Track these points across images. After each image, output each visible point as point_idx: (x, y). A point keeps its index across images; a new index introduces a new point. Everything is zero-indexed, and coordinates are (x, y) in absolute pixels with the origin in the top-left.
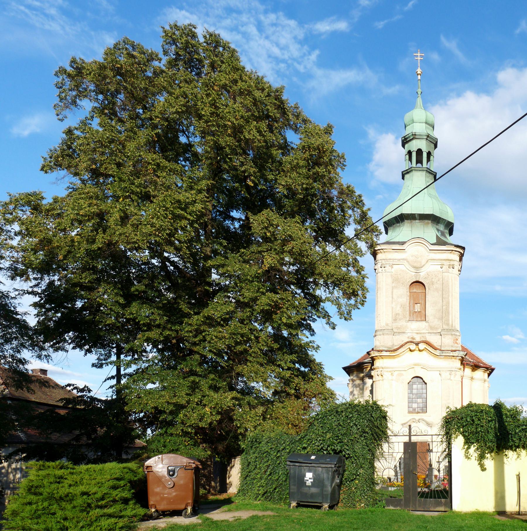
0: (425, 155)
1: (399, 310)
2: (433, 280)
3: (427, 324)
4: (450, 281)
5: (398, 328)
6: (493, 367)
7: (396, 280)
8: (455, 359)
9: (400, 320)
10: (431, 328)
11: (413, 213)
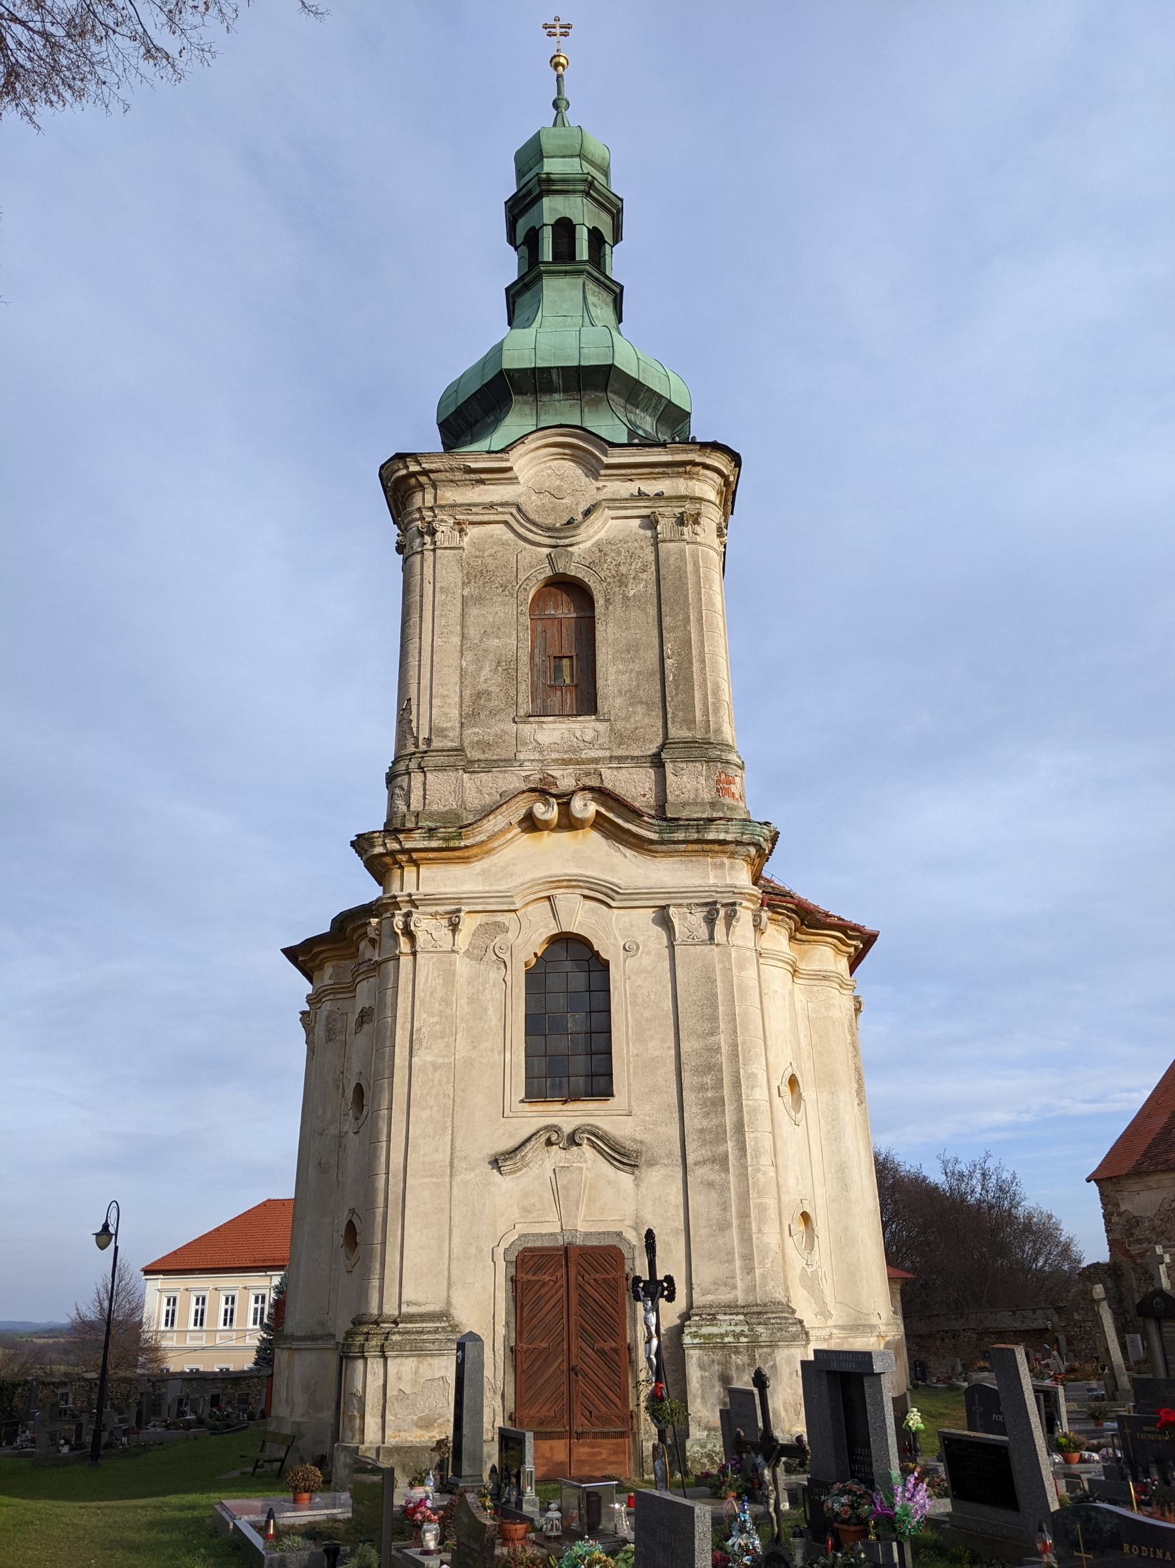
0: (582, 236)
1: (488, 677)
2: (623, 569)
3: (602, 727)
4: (690, 568)
5: (484, 745)
6: (870, 927)
7: (475, 573)
8: (732, 855)
9: (493, 713)
10: (620, 738)
11: (541, 364)
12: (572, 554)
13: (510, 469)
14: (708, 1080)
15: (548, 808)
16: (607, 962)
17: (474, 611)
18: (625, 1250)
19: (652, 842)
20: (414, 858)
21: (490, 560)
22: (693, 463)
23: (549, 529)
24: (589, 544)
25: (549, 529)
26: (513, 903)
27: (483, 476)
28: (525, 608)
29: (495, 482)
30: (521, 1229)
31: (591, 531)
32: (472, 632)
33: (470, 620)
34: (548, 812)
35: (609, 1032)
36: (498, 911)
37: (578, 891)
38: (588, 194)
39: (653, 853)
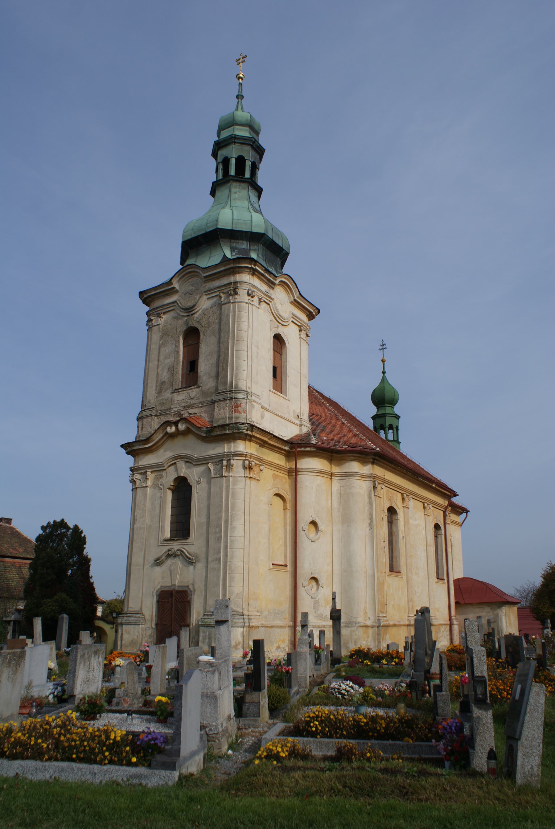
0: (233, 161)
10: (204, 394)
14: (217, 530)
16: (191, 486)
17: (162, 349)
18: (189, 592)
21: (169, 326)
22: (232, 268)
26: (164, 467)
30: (161, 584)
31: (200, 307)
32: (161, 358)
33: (161, 353)
36: (158, 469)
37: (183, 460)
38: (235, 142)
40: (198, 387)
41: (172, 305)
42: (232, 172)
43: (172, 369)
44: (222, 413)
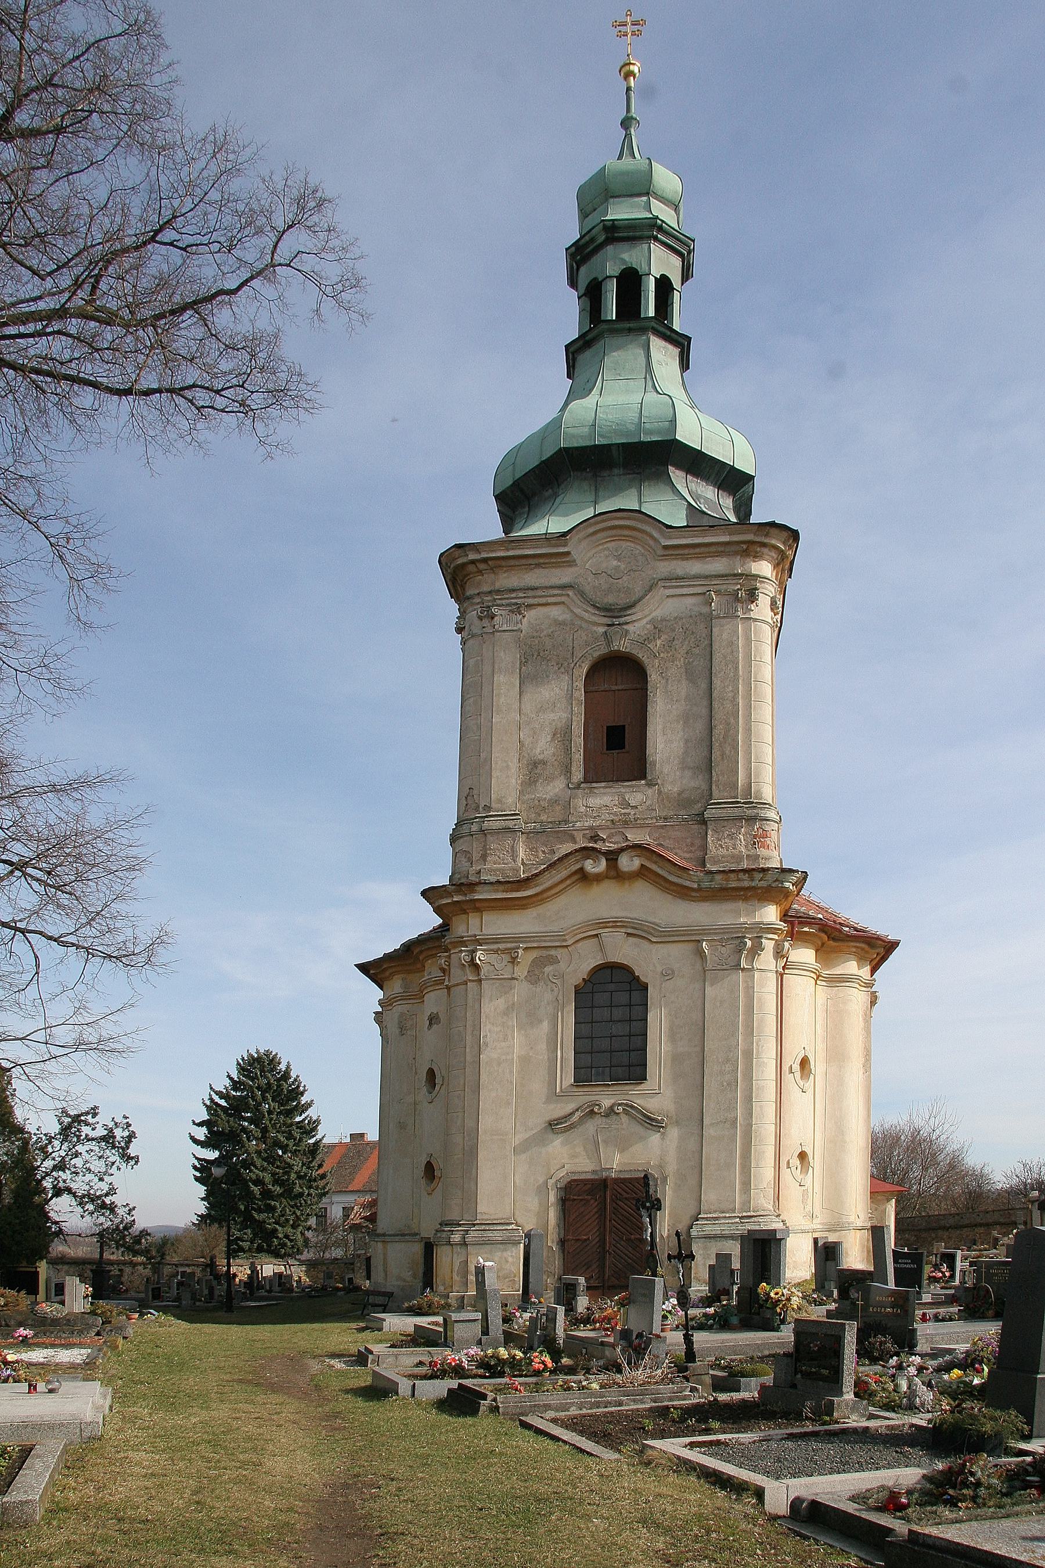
12: (627, 631)
13: (568, 553)
15: (598, 862)
19: (693, 890)
20: (479, 907)
23: (606, 610)
24: (645, 621)
25: (606, 610)
27: (542, 561)
28: (580, 684)
29: (557, 565)
31: (646, 612)
34: (595, 866)
35: (645, 1034)
39: (694, 899)
40: (650, 784)
41: (556, 592)
42: (611, 311)
43: (564, 735)
44: (726, 848)
